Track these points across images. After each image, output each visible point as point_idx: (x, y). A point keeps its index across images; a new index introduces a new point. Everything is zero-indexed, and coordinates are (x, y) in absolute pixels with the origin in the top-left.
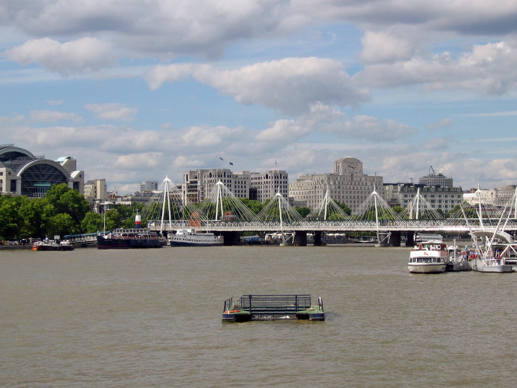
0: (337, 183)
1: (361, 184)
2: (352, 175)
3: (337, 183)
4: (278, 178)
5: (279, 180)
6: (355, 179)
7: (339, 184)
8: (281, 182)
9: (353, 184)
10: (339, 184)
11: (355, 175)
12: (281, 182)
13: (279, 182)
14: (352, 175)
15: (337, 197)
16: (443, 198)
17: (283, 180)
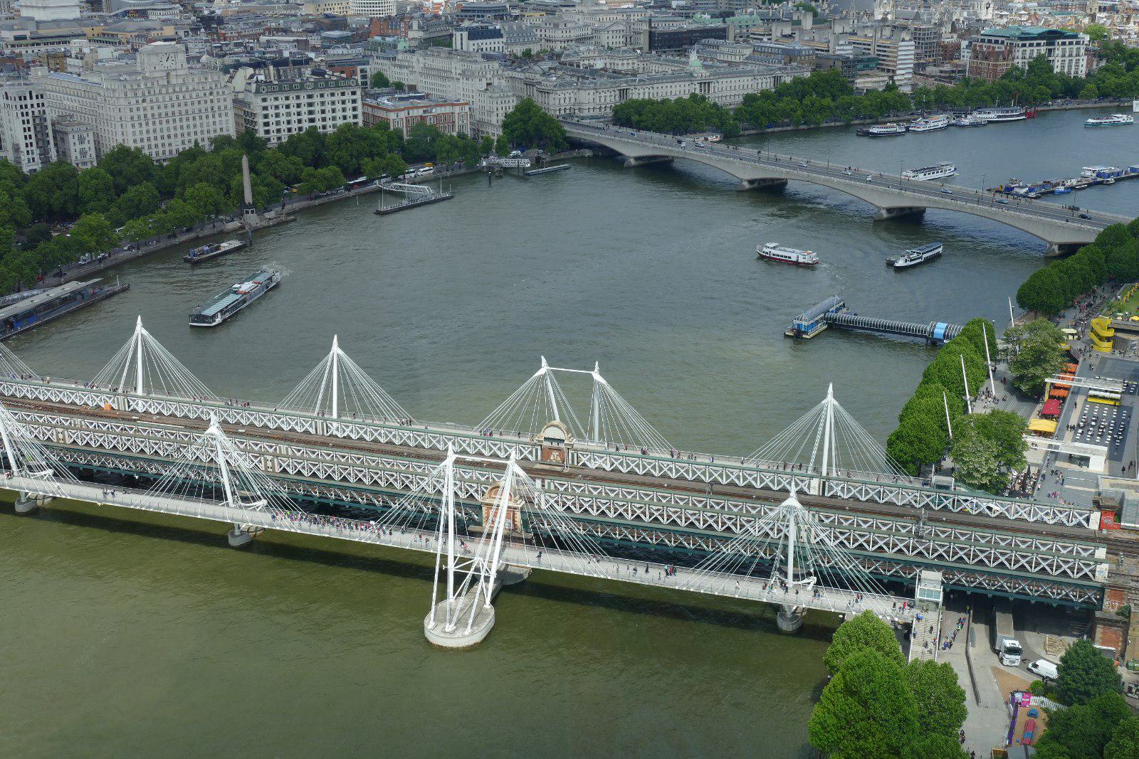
0: (139, 93)
1: (184, 89)
2: (168, 75)
3: (139, 93)
4: (25, 98)
5: (29, 102)
6: (173, 81)
7: (144, 94)
8: (32, 106)
9: (171, 90)
10: (144, 94)
11: (173, 73)
12: (32, 106)
13: (29, 106)
14: (168, 75)
15: (142, 117)
16: (327, 99)
17: (35, 101)
